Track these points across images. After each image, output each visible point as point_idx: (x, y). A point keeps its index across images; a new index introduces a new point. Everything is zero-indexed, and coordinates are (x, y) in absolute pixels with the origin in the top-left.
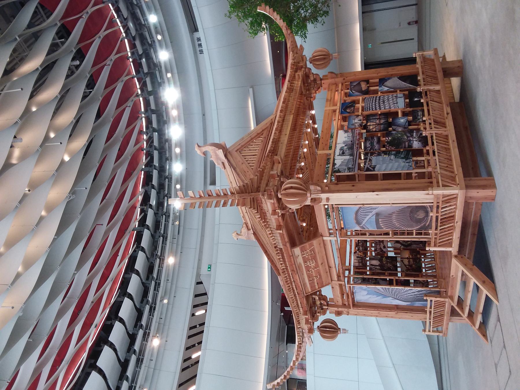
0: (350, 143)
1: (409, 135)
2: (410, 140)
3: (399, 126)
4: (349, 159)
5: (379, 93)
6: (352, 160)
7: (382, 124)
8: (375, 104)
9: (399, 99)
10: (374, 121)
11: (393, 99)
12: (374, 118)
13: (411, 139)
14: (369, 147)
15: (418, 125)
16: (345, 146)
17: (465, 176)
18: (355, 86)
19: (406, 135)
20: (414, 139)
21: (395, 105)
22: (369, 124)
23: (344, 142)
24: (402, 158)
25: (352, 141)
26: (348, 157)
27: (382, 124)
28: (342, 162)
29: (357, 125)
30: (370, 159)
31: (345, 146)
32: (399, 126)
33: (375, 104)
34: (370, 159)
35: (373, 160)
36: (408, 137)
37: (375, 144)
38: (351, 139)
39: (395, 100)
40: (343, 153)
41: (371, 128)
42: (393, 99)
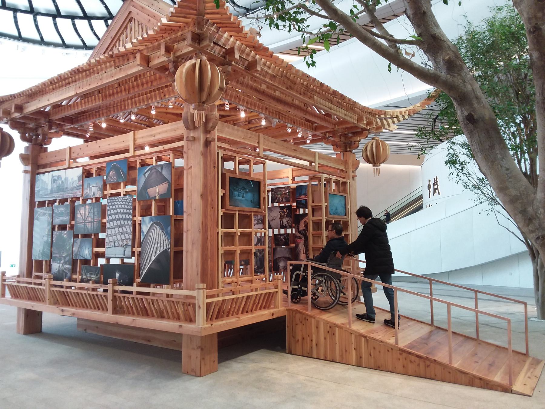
0: (65, 187)
1: (67, 259)
2: (60, 260)
3: (80, 247)
4: (47, 189)
5: (140, 218)
6: (46, 193)
7: (85, 225)
8: (117, 213)
9: (122, 249)
10: (91, 214)
11: (122, 240)
12: (96, 214)
13: (62, 262)
14: (58, 211)
15: (81, 274)
16: (62, 181)
17: (220, 334)
18: (161, 173)
19: (67, 256)
20: (61, 265)
21: (112, 244)
22: (87, 207)
23: (66, 179)
24: (43, 249)
25: (67, 188)
26: (49, 188)
27: (85, 225)
28: (45, 182)
29: (88, 190)
30: (45, 214)
31: (62, 181)
32: (80, 247)
33: (117, 213)
34: (45, 214)
35: (44, 217)
36: (65, 257)
37: (61, 218)
38: (70, 186)
39: (121, 243)
40: (54, 181)
41: (81, 212)
42: (122, 240)
